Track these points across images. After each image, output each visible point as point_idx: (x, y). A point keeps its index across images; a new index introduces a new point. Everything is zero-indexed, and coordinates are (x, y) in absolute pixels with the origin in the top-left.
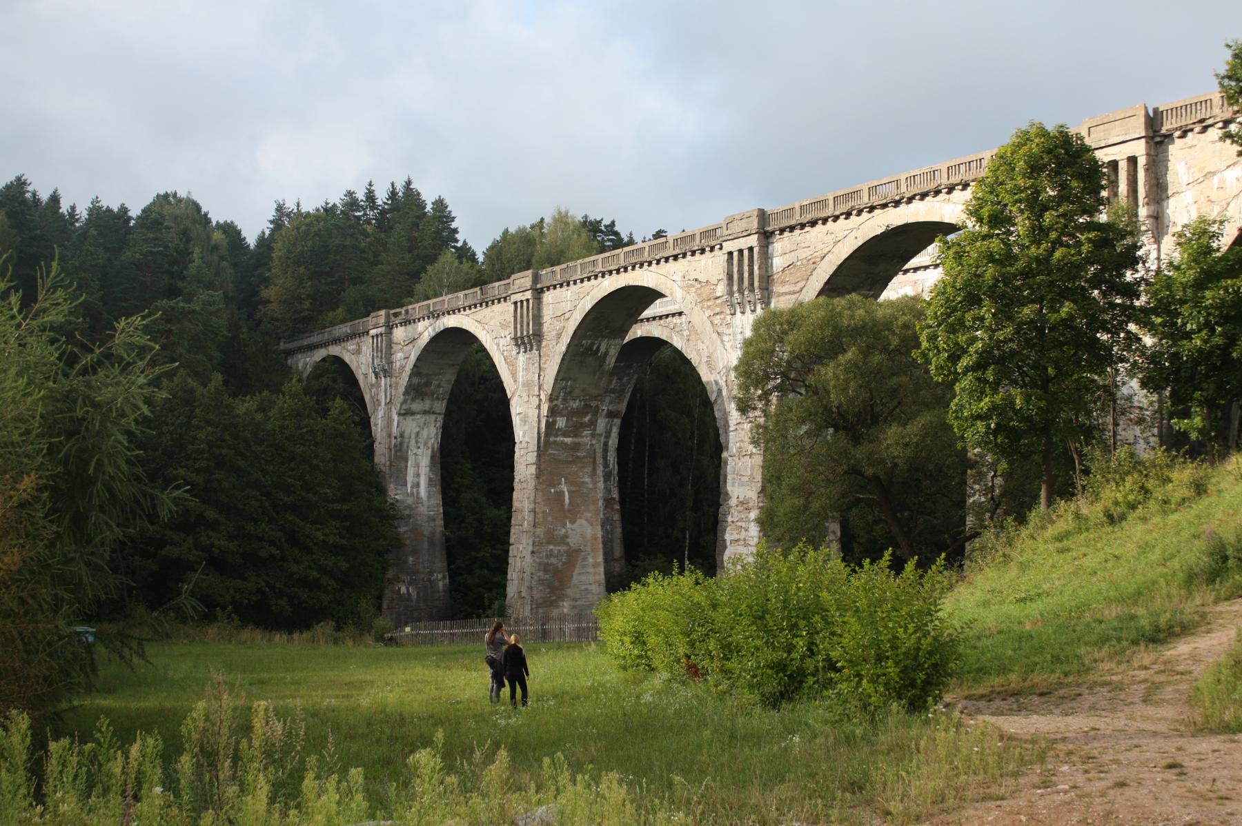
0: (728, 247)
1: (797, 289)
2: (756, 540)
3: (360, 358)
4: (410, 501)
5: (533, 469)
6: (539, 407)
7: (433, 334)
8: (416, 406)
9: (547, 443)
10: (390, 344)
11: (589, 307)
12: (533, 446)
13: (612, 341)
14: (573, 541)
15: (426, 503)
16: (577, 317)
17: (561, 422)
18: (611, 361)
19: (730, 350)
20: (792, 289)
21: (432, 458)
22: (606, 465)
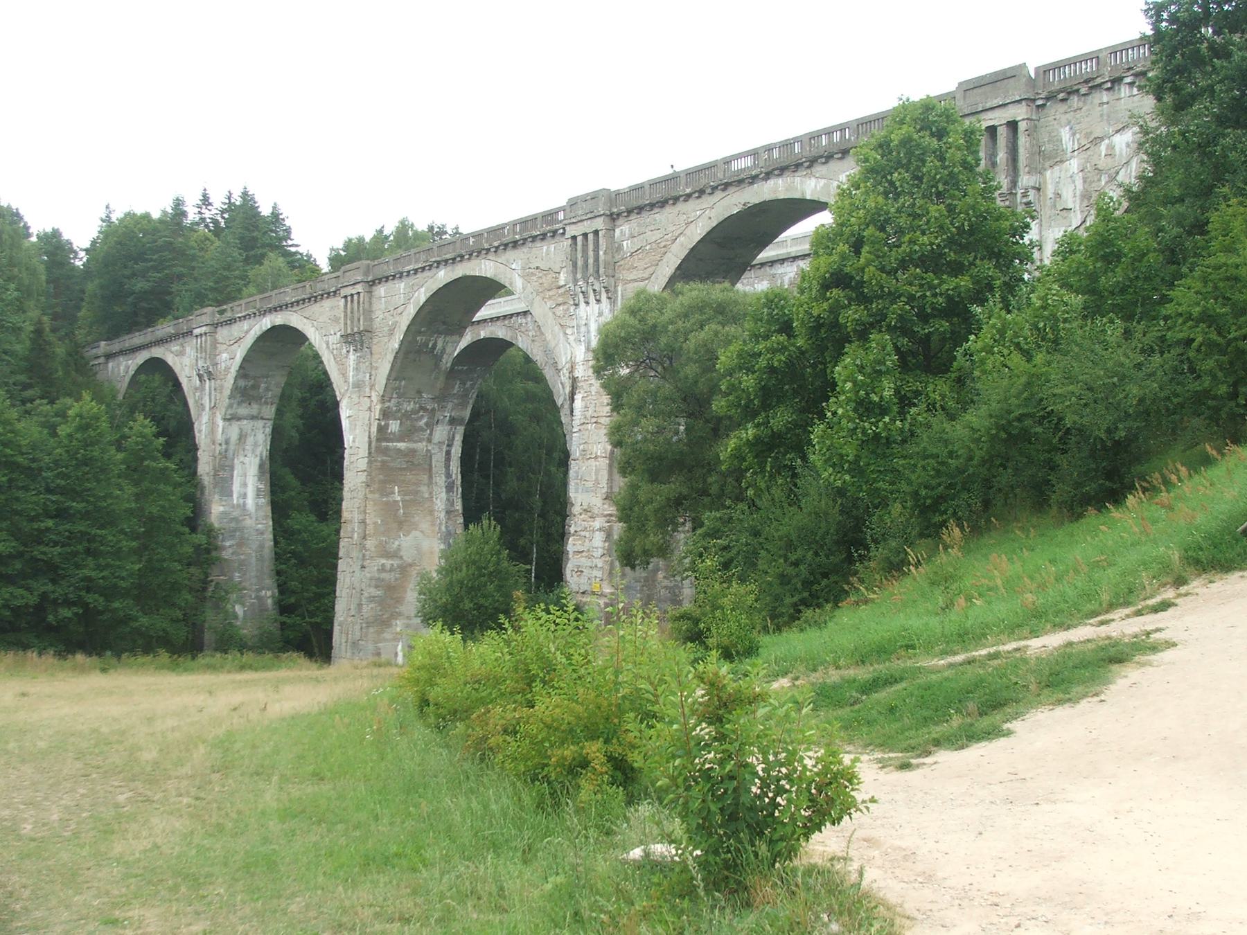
0: (571, 230)
1: (646, 275)
2: (600, 552)
3: (184, 361)
4: (236, 513)
5: (363, 477)
6: (370, 408)
7: (259, 333)
8: (243, 411)
9: (378, 449)
10: (215, 343)
11: (423, 299)
12: (364, 452)
14: (408, 555)
15: (254, 516)
16: (411, 311)
17: (394, 426)
18: (447, 362)
19: (573, 344)
20: (641, 274)
21: (261, 466)
22: (448, 475)
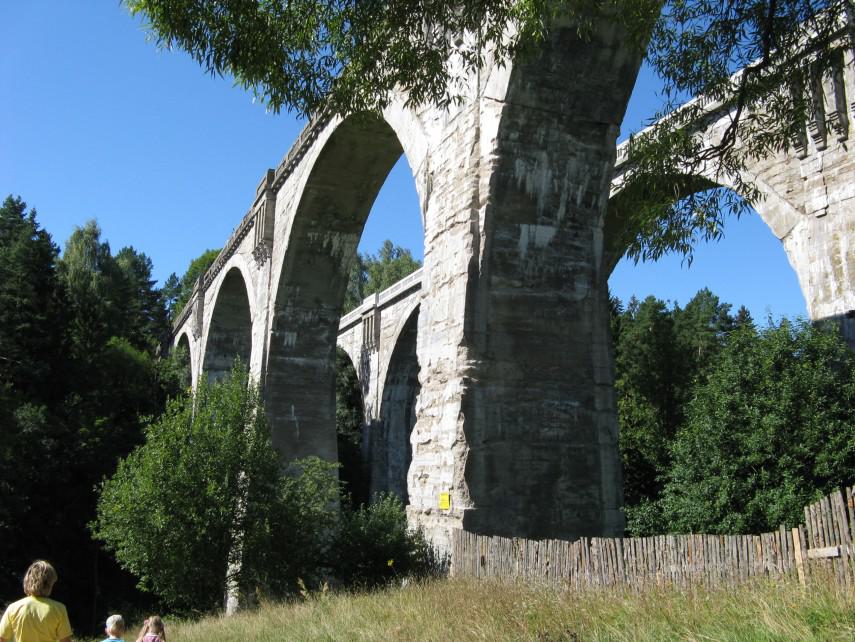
2: (453, 437)
8: (219, 362)
13: (345, 237)
17: (291, 339)
